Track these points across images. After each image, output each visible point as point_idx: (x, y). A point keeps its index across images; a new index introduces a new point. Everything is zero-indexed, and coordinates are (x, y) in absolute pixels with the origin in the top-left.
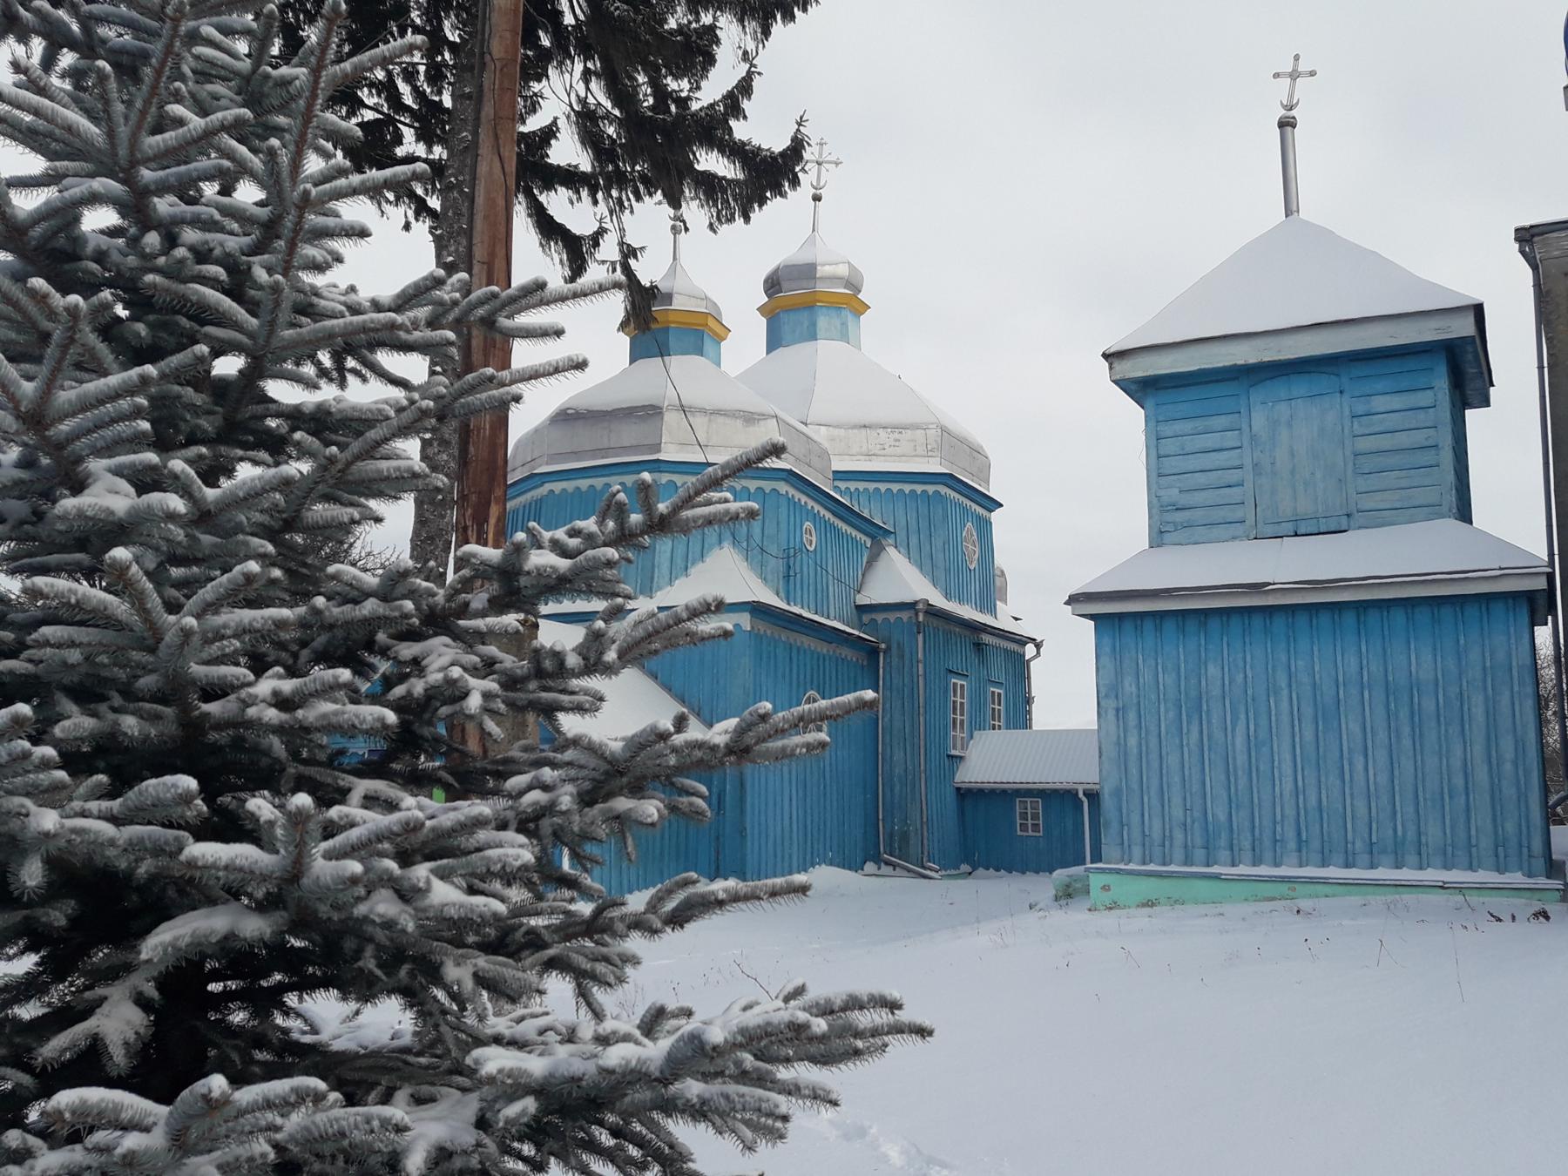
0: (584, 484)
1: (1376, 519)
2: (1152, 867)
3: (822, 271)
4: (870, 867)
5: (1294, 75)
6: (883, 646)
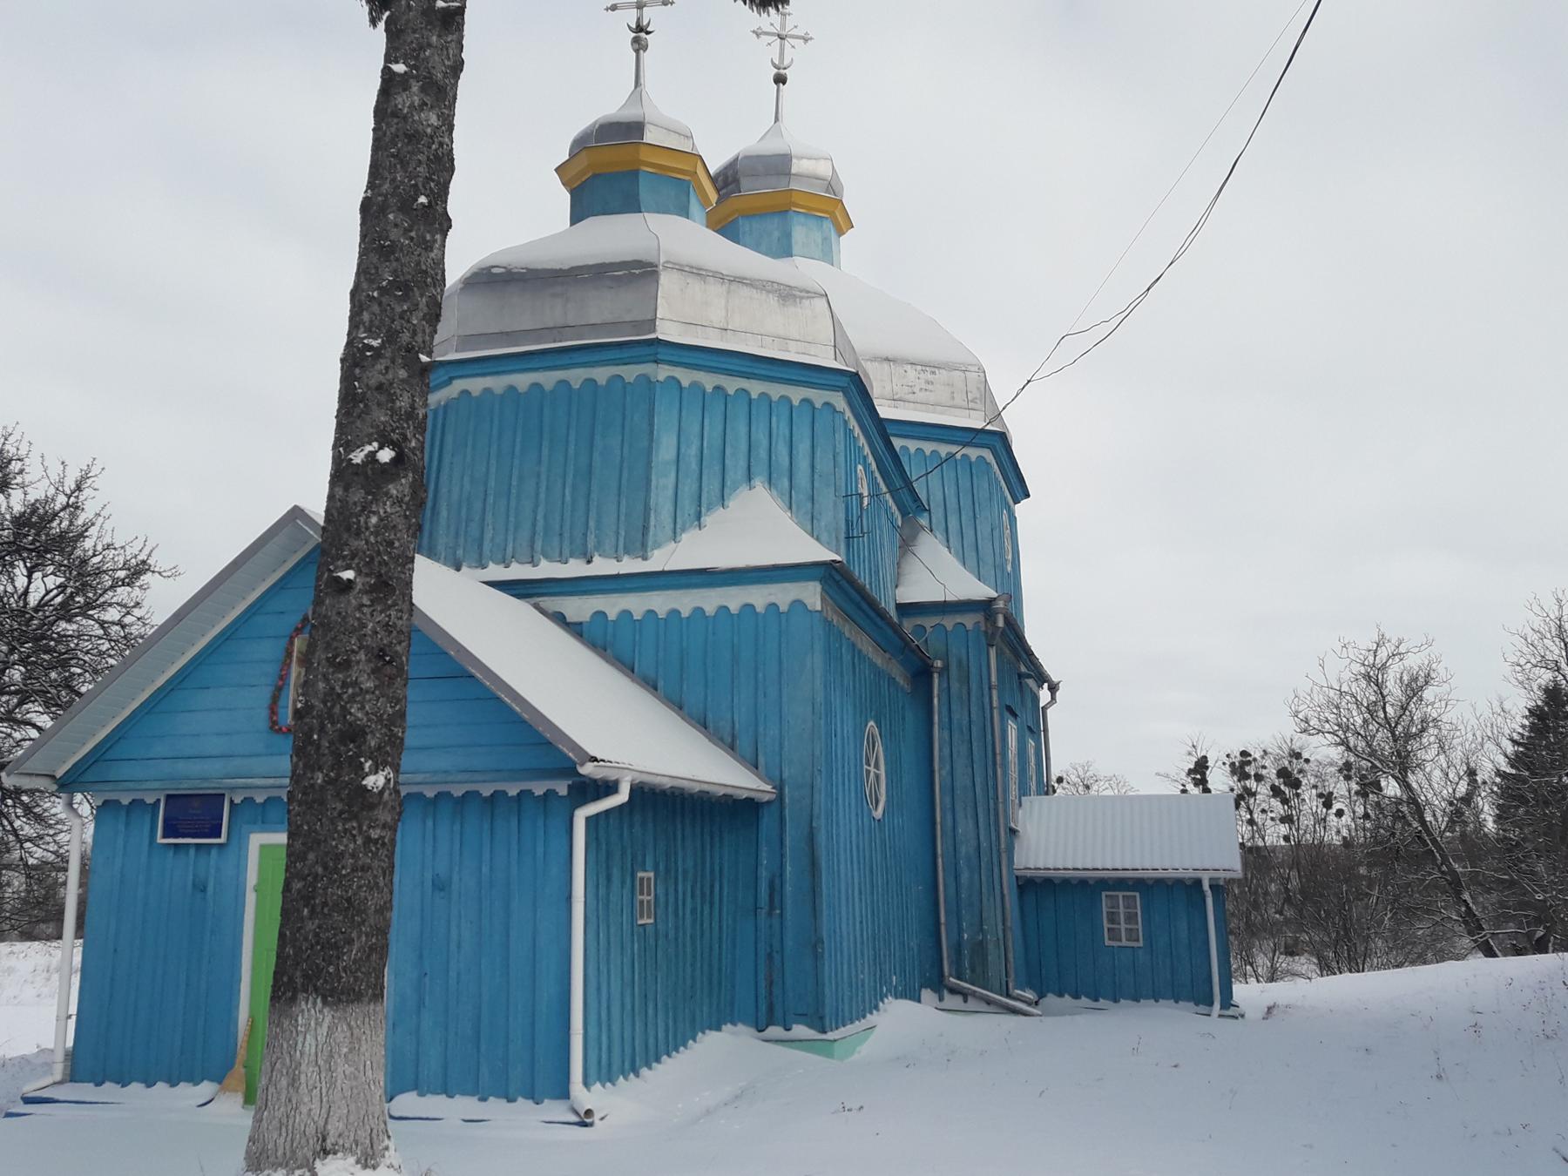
0: (522, 381)
3: (797, 167)
6: (939, 664)
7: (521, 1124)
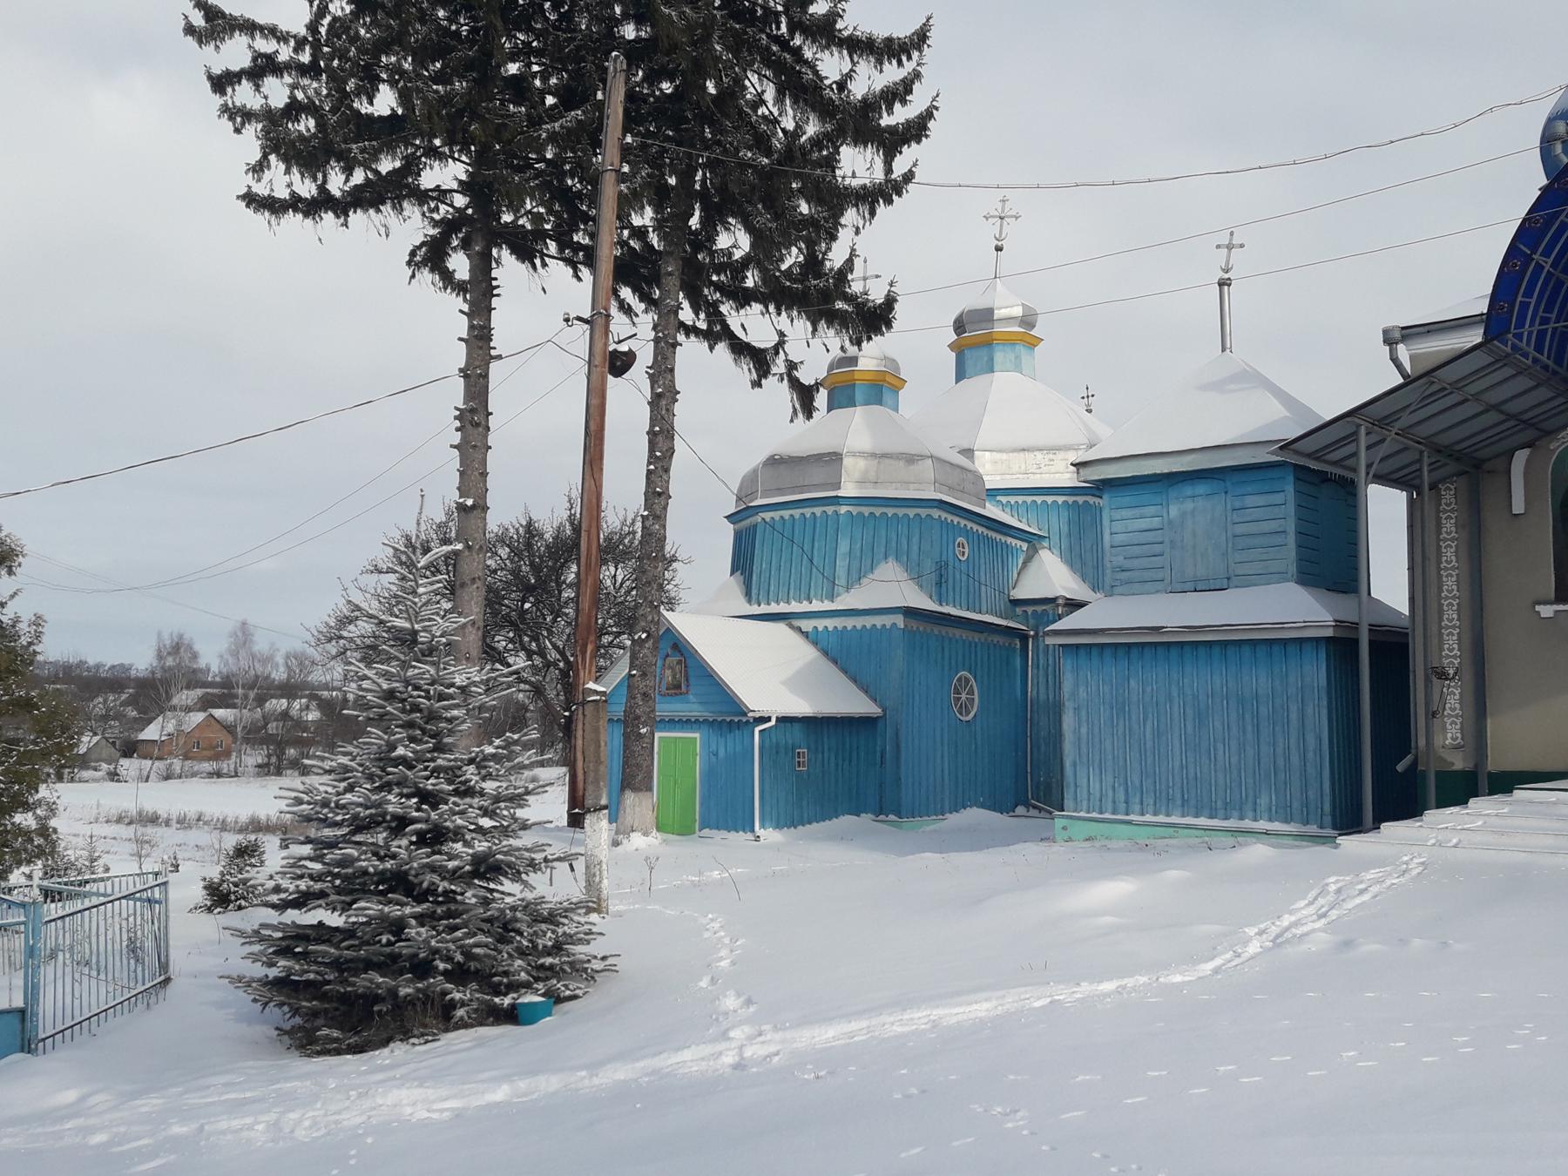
1: (1247, 581)
2: (1094, 815)
3: (998, 314)
4: (1020, 810)
5: (1230, 247)
7: (739, 838)
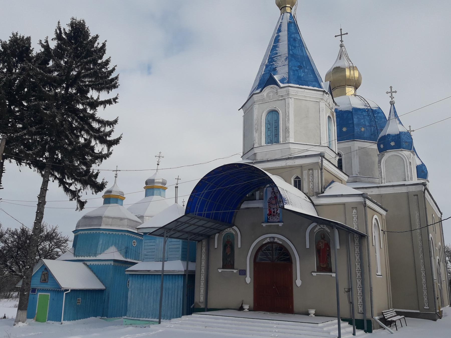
0: (86, 232)
2: (132, 318)
5: (178, 179)
